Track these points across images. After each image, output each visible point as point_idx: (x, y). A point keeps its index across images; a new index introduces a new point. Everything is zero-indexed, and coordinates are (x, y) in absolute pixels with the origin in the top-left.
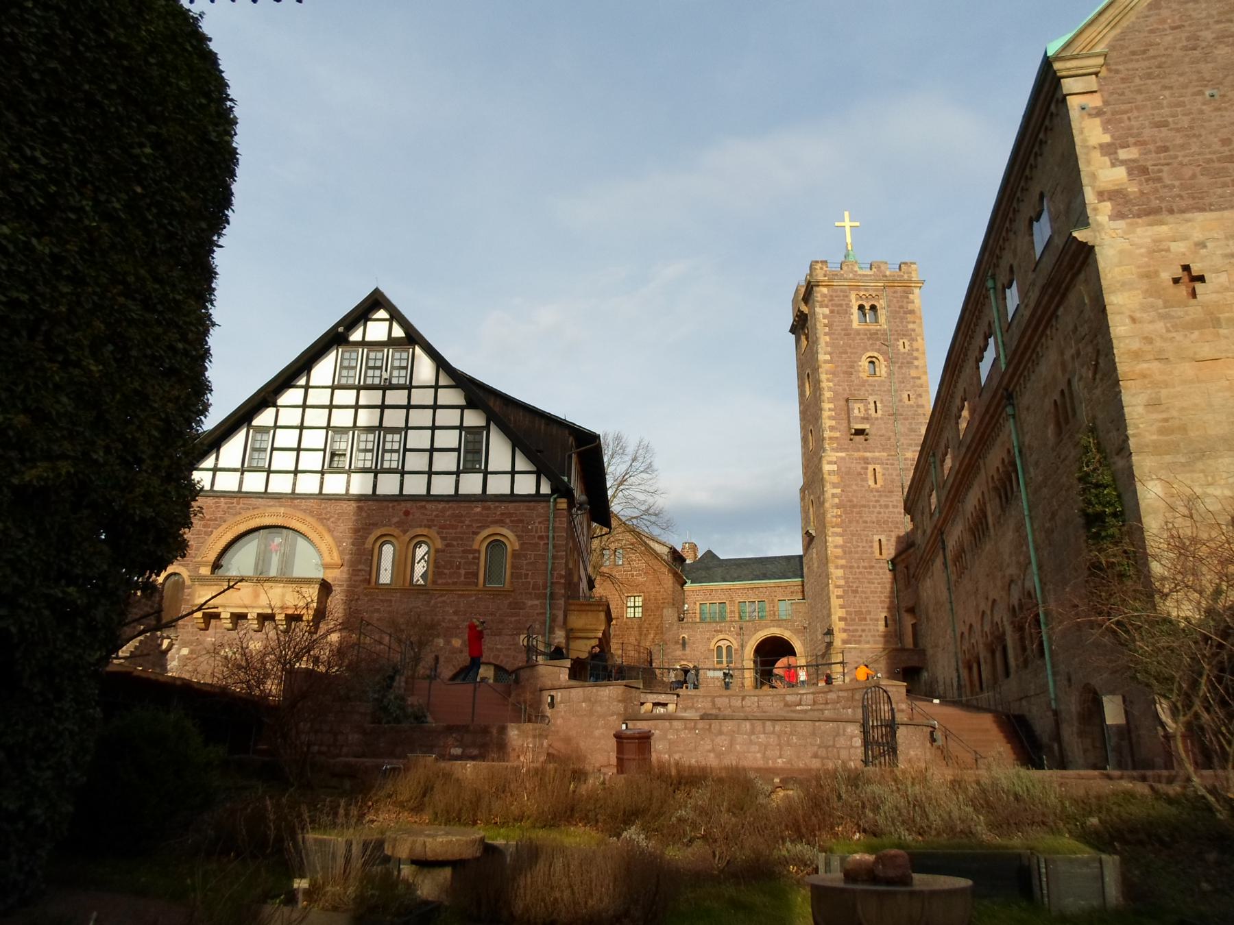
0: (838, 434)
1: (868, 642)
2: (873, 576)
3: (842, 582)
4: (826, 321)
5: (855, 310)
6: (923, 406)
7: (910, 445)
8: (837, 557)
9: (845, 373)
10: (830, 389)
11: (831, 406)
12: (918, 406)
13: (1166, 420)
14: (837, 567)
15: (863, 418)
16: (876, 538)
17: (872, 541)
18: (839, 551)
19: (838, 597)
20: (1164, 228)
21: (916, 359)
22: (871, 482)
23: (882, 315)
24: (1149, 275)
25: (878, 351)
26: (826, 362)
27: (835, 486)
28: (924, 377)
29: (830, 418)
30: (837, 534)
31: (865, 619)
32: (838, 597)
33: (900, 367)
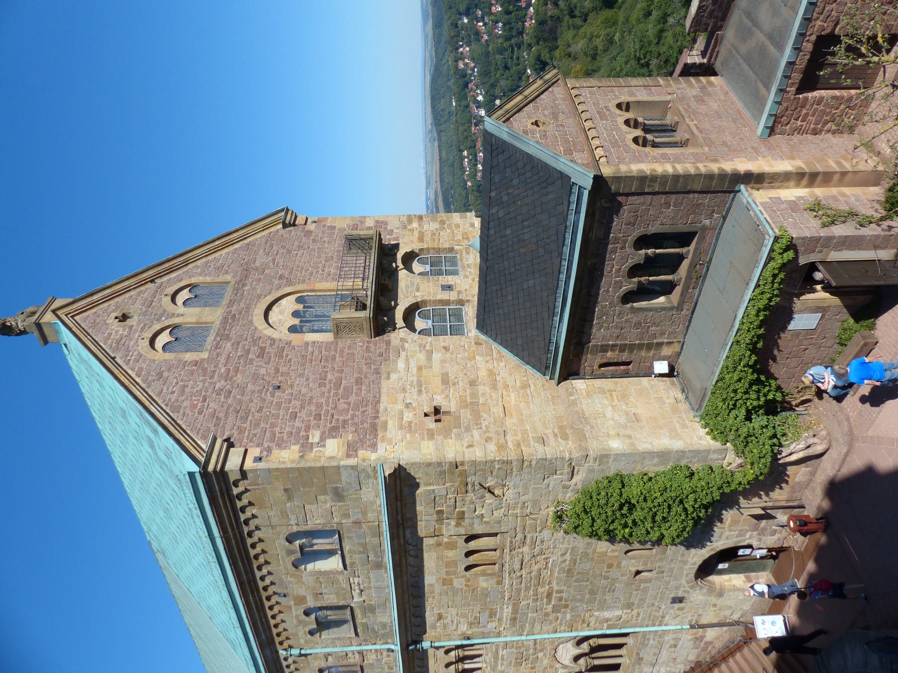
13: (555, 435)
20: (390, 423)
24: (431, 435)
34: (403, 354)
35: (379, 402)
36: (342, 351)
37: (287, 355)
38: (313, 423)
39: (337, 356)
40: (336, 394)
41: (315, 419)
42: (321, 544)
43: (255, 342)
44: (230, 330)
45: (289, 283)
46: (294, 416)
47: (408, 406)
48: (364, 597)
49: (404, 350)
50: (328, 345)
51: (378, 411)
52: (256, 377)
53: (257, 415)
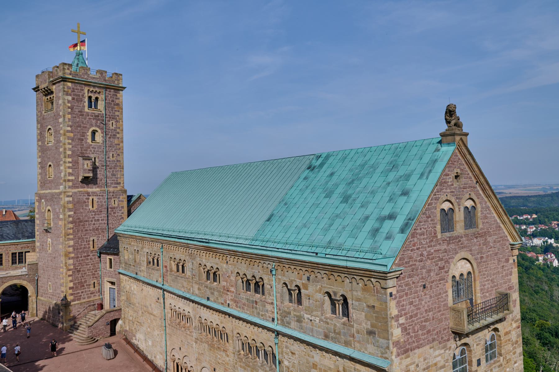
0: (73, 178)
1: (84, 298)
2: (89, 261)
3: (72, 267)
4: (69, 105)
5: (86, 100)
6: (120, 161)
7: (112, 184)
8: (70, 253)
9: (79, 139)
10: (70, 149)
11: (70, 160)
12: (117, 161)
14: (69, 259)
15: (89, 170)
16: (92, 239)
17: (89, 241)
18: (71, 249)
19: (69, 276)
20: (409, 359)
21: (118, 133)
22: (90, 207)
23: (101, 105)
25: (99, 127)
26: (68, 131)
27: (70, 210)
28: (121, 144)
29: (69, 167)
30: (69, 239)
31: (84, 286)
32: (69, 276)
33: (110, 138)
34: (443, 351)
35: (419, 348)
36: (443, 314)
37: (440, 284)
38: (408, 315)
39: (441, 313)
40: (422, 322)
41: (410, 316)
42: (339, 308)
43: (447, 262)
44: (453, 243)
45: (478, 266)
46: (411, 303)
47: (417, 366)
48: (307, 320)
49: (445, 351)
50: (446, 305)
51: (414, 349)
52: (429, 271)
53: (411, 282)
